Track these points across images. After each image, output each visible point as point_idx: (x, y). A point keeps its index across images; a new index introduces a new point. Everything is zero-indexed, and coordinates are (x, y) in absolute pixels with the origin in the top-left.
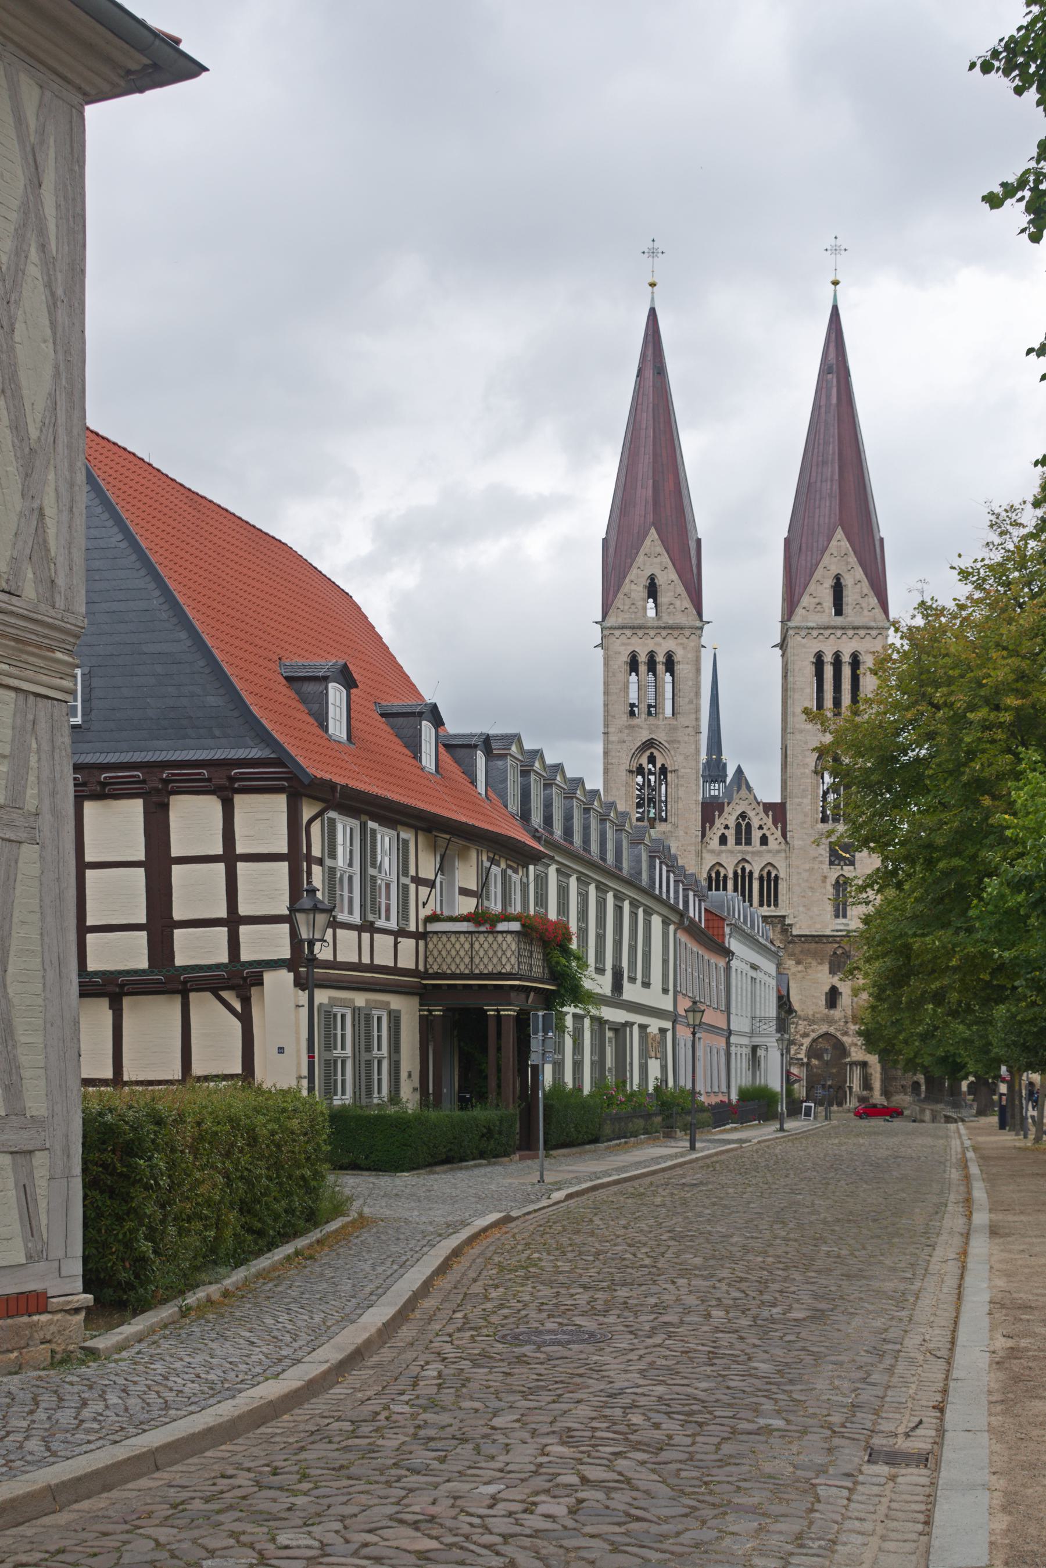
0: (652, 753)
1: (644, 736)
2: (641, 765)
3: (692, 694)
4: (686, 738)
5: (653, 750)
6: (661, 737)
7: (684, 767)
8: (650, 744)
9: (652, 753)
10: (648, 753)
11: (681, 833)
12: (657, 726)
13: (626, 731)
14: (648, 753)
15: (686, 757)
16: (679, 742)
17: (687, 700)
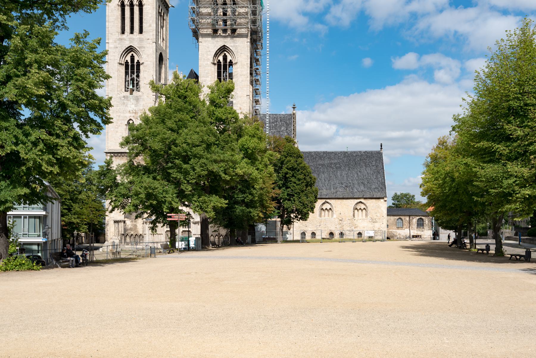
0: (132, 54)
1: (127, 44)
2: (127, 61)
3: (151, 21)
4: (148, 45)
5: (132, 53)
6: (135, 45)
7: (147, 61)
8: (130, 49)
9: (132, 54)
10: (130, 54)
11: (145, 97)
12: (133, 39)
13: (118, 42)
14: (130, 54)
15: (148, 55)
16: (144, 47)
17: (148, 25)
